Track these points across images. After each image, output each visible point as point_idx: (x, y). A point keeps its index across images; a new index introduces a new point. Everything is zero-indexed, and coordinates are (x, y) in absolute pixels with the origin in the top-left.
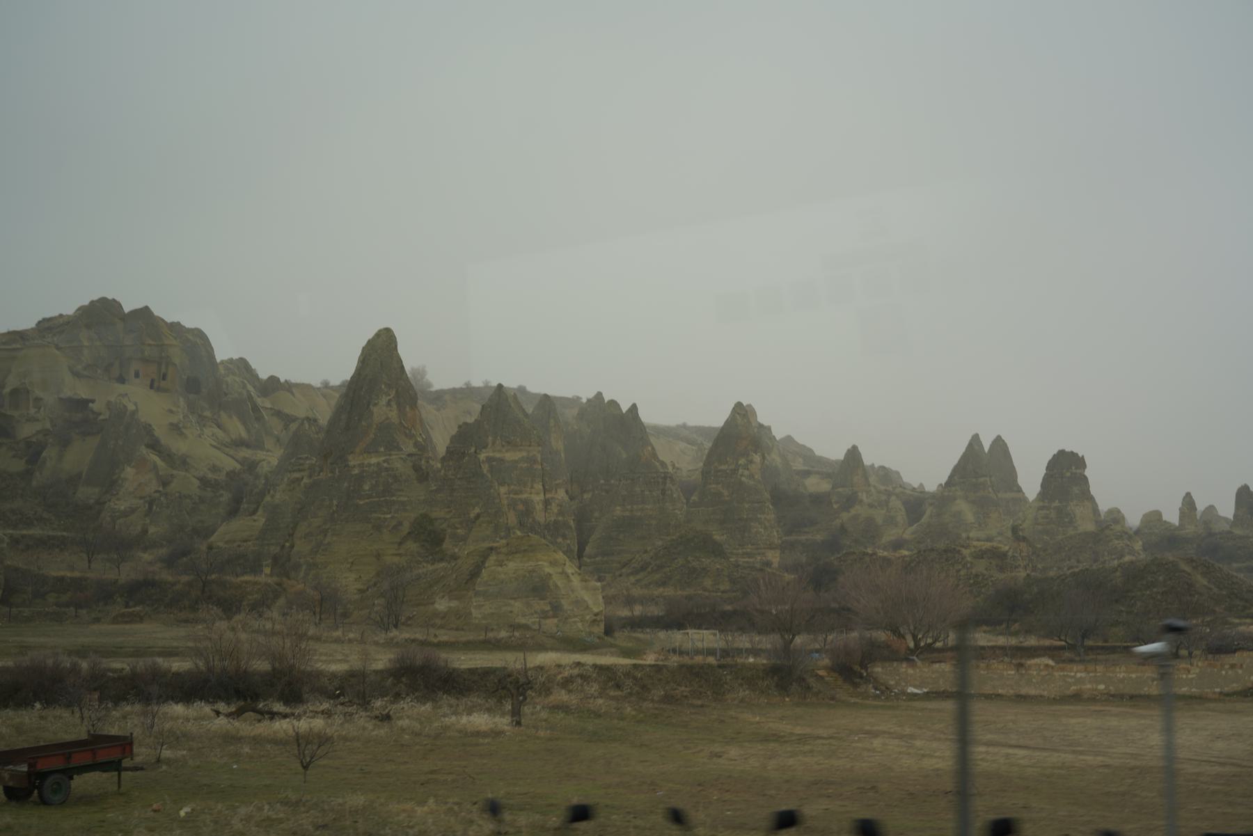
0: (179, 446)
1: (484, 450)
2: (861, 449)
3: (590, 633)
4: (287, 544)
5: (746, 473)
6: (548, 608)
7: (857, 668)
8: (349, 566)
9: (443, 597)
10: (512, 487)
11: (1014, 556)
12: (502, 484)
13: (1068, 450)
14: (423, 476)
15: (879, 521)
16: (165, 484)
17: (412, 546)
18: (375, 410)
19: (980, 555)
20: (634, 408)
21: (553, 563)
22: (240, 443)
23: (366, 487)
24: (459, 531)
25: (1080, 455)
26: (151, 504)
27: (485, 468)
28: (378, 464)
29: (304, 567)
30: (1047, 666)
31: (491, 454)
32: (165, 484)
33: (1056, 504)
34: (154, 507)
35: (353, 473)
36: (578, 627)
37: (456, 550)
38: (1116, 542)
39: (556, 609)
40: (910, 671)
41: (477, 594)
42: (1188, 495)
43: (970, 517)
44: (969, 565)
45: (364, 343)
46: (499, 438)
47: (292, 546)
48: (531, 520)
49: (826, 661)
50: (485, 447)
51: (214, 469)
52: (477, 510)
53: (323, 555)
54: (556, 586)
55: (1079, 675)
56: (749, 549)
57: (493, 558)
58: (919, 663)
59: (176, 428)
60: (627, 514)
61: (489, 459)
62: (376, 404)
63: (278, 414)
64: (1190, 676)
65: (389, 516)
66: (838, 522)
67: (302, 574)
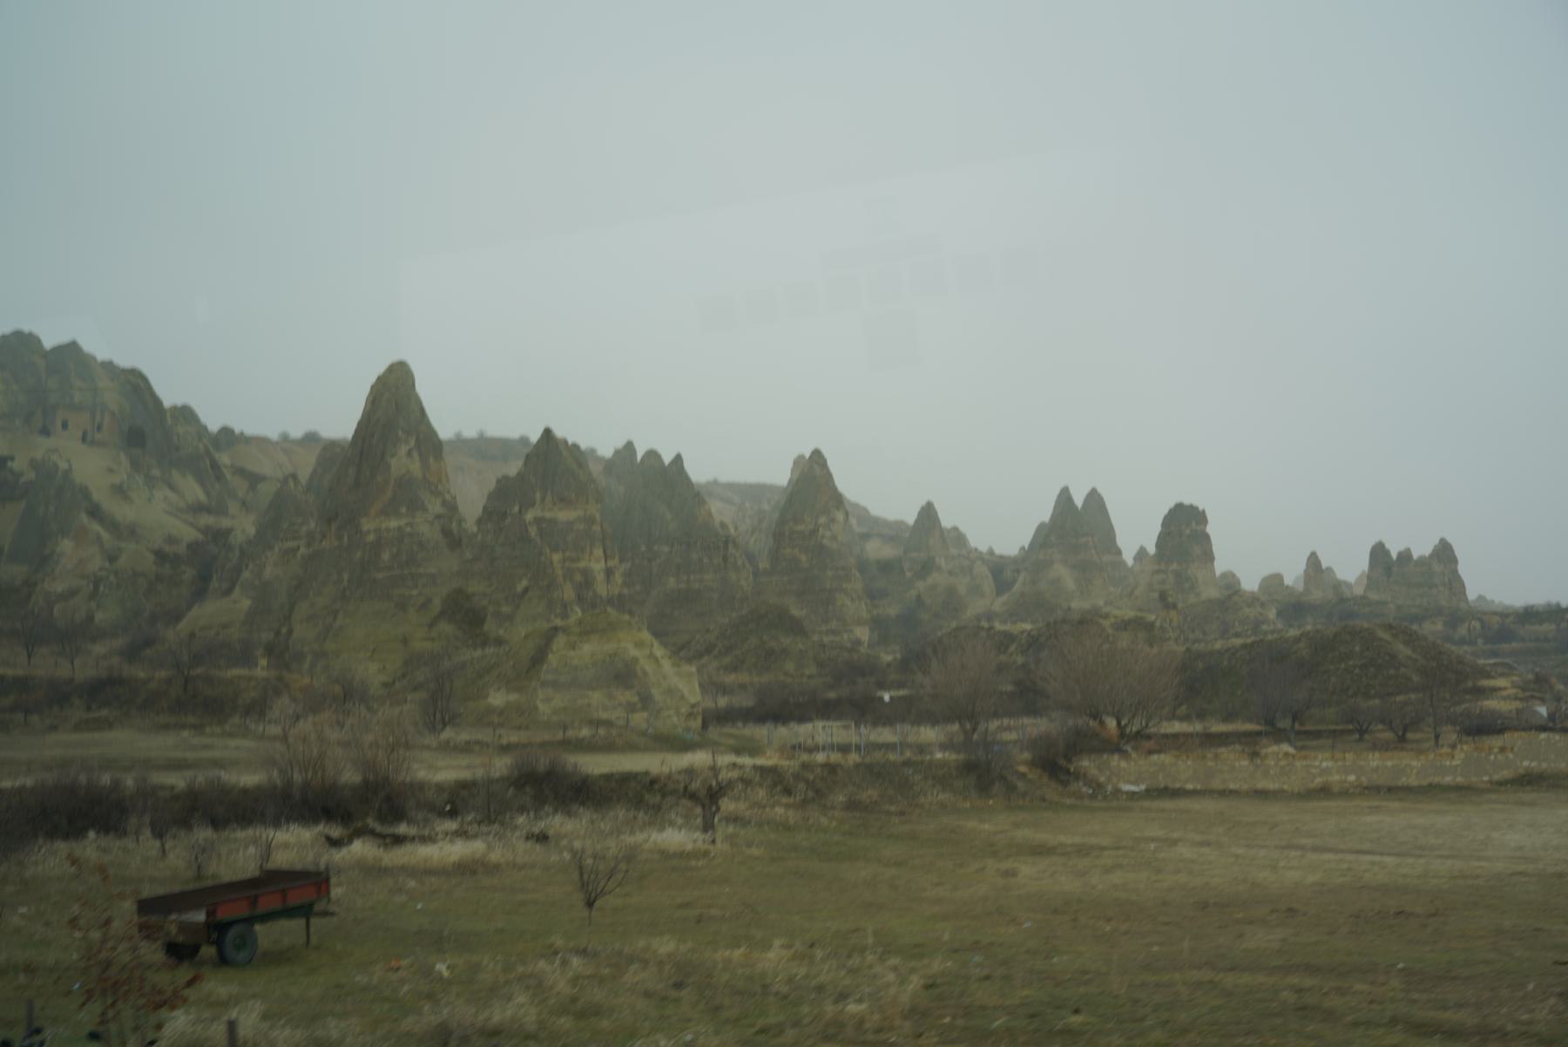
0: (123, 512)
2: (937, 506)
3: (688, 729)
4: (284, 630)
5: (828, 534)
6: (636, 699)
7: (1062, 762)
9: (499, 689)
10: (568, 554)
11: (1162, 627)
12: (555, 549)
13: (1187, 502)
14: (454, 541)
15: (962, 590)
16: (112, 559)
17: (446, 628)
18: (393, 462)
19: (1124, 625)
20: (678, 459)
21: (640, 644)
22: (198, 508)
23: (386, 556)
25: (1201, 508)
26: (96, 584)
27: (533, 531)
28: (400, 529)
29: (309, 658)
30: (1286, 754)
32: (112, 559)
33: (1174, 566)
34: (102, 588)
36: (672, 721)
37: (501, 632)
38: (1247, 610)
39: (646, 701)
40: (1123, 764)
41: (544, 684)
42: (1313, 556)
43: (1070, 583)
44: (1111, 639)
45: (373, 379)
47: (290, 632)
48: (591, 594)
49: (1026, 755)
50: (533, 504)
51: (171, 540)
52: (525, 583)
54: (645, 673)
55: (1324, 764)
56: (834, 625)
57: (560, 641)
58: (1134, 755)
59: (120, 491)
60: (683, 586)
62: (393, 456)
63: (241, 472)
64: (1454, 763)
65: (415, 592)
66: (913, 593)
67: (306, 665)
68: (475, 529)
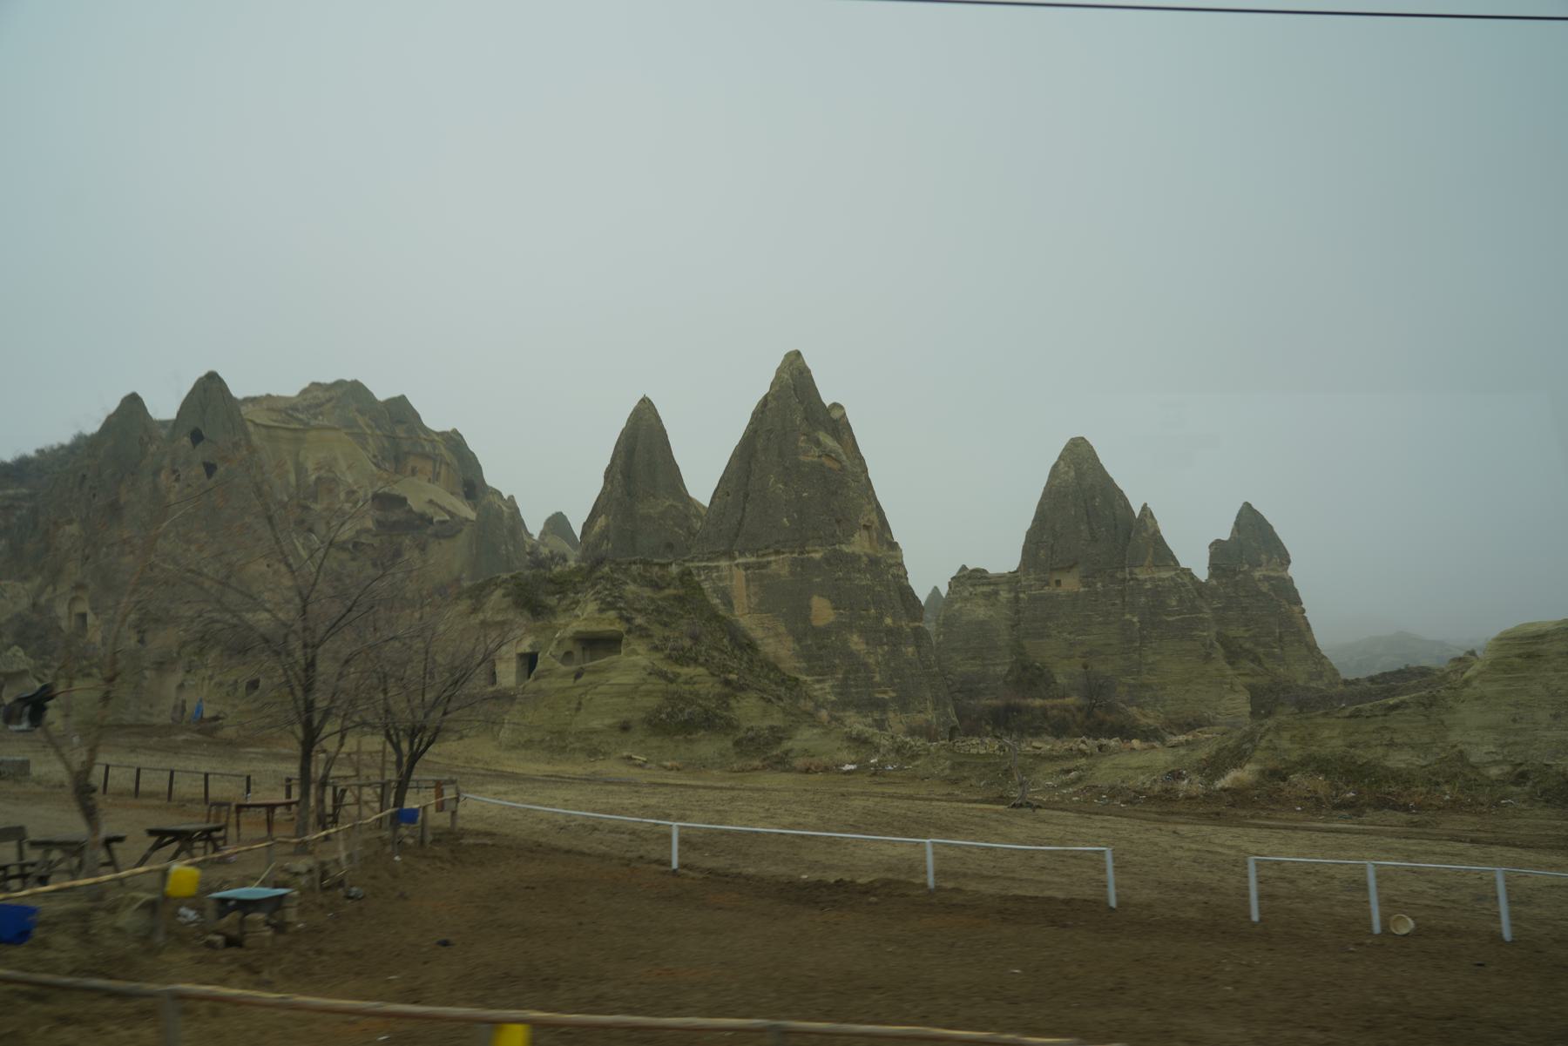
1: (1259, 569)
8: (1228, 686)
24: (1276, 650)
27: (1264, 587)
28: (1172, 579)
31: (1265, 573)
35: (1147, 587)
46: (1276, 556)
50: (1260, 566)
53: (1155, 675)
61: (1267, 578)
68: (1214, 582)
